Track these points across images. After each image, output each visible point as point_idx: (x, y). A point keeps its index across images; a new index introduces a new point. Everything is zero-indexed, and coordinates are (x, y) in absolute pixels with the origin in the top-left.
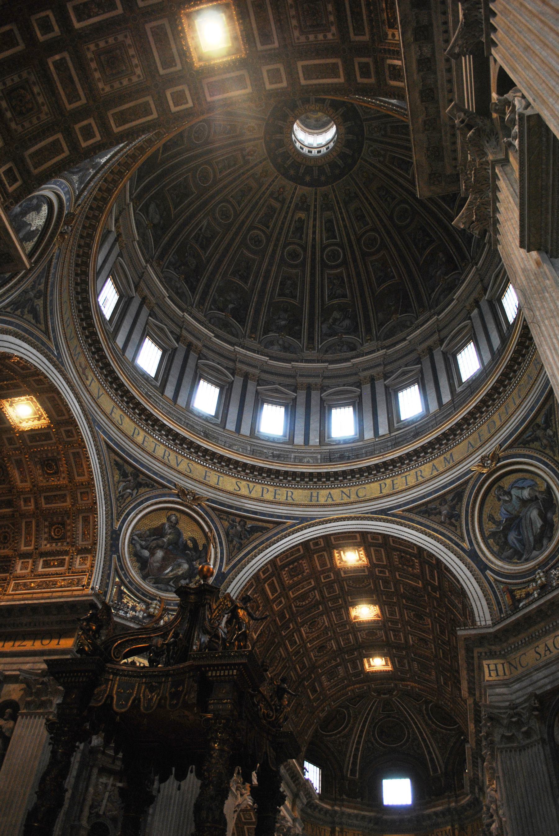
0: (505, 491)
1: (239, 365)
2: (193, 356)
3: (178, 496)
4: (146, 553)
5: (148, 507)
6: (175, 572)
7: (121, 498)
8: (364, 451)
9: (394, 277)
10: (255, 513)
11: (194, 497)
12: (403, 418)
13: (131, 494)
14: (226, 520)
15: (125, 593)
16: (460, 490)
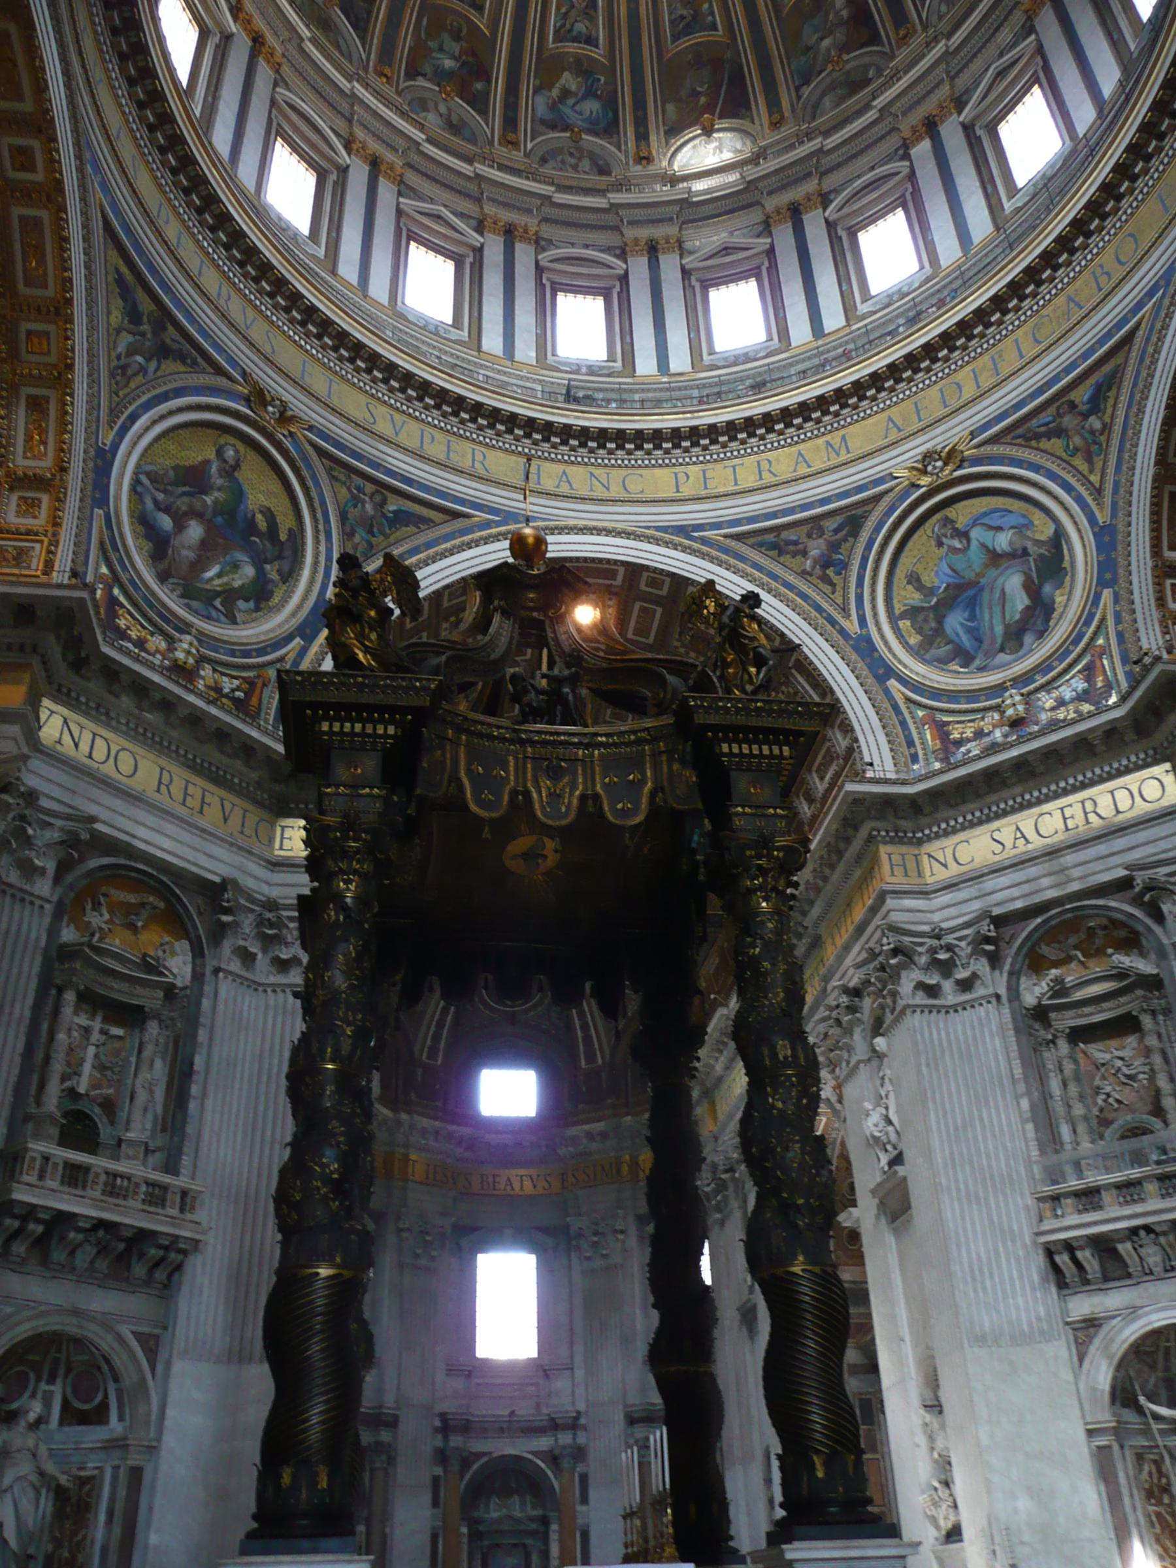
0: (956, 530)
1: (360, 133)
2: (264, 73)
3: (247, 401)
4: (166, 522)
5: (180, 410)
6: (225, 579)
7: (121, 372)
8: (637, 397)
9: (714, 27)
10: (409, 481)
11: (282, 413)
12: (719, 346)
13: (143, 370)
14: (344, 483)
15: (122, 606)
16: (859, 511)
